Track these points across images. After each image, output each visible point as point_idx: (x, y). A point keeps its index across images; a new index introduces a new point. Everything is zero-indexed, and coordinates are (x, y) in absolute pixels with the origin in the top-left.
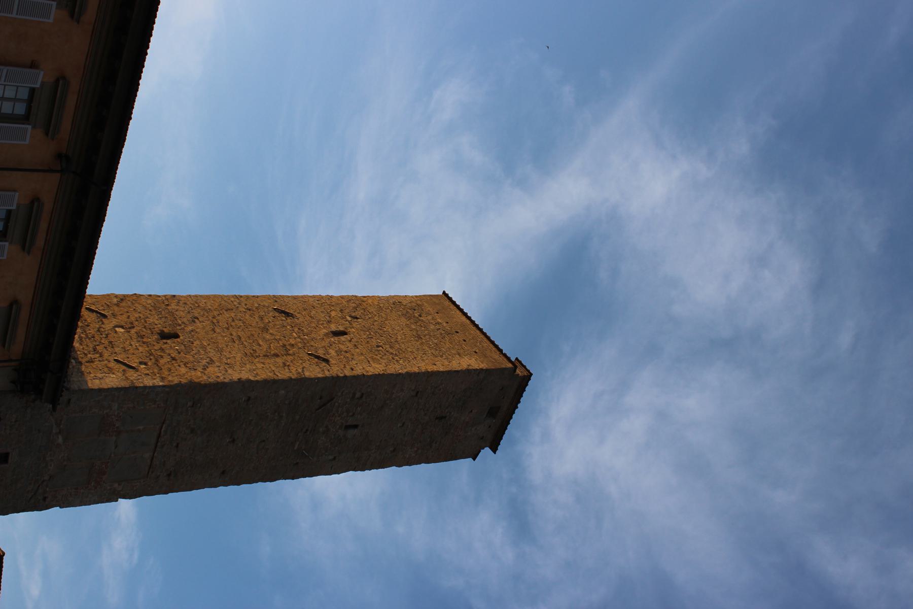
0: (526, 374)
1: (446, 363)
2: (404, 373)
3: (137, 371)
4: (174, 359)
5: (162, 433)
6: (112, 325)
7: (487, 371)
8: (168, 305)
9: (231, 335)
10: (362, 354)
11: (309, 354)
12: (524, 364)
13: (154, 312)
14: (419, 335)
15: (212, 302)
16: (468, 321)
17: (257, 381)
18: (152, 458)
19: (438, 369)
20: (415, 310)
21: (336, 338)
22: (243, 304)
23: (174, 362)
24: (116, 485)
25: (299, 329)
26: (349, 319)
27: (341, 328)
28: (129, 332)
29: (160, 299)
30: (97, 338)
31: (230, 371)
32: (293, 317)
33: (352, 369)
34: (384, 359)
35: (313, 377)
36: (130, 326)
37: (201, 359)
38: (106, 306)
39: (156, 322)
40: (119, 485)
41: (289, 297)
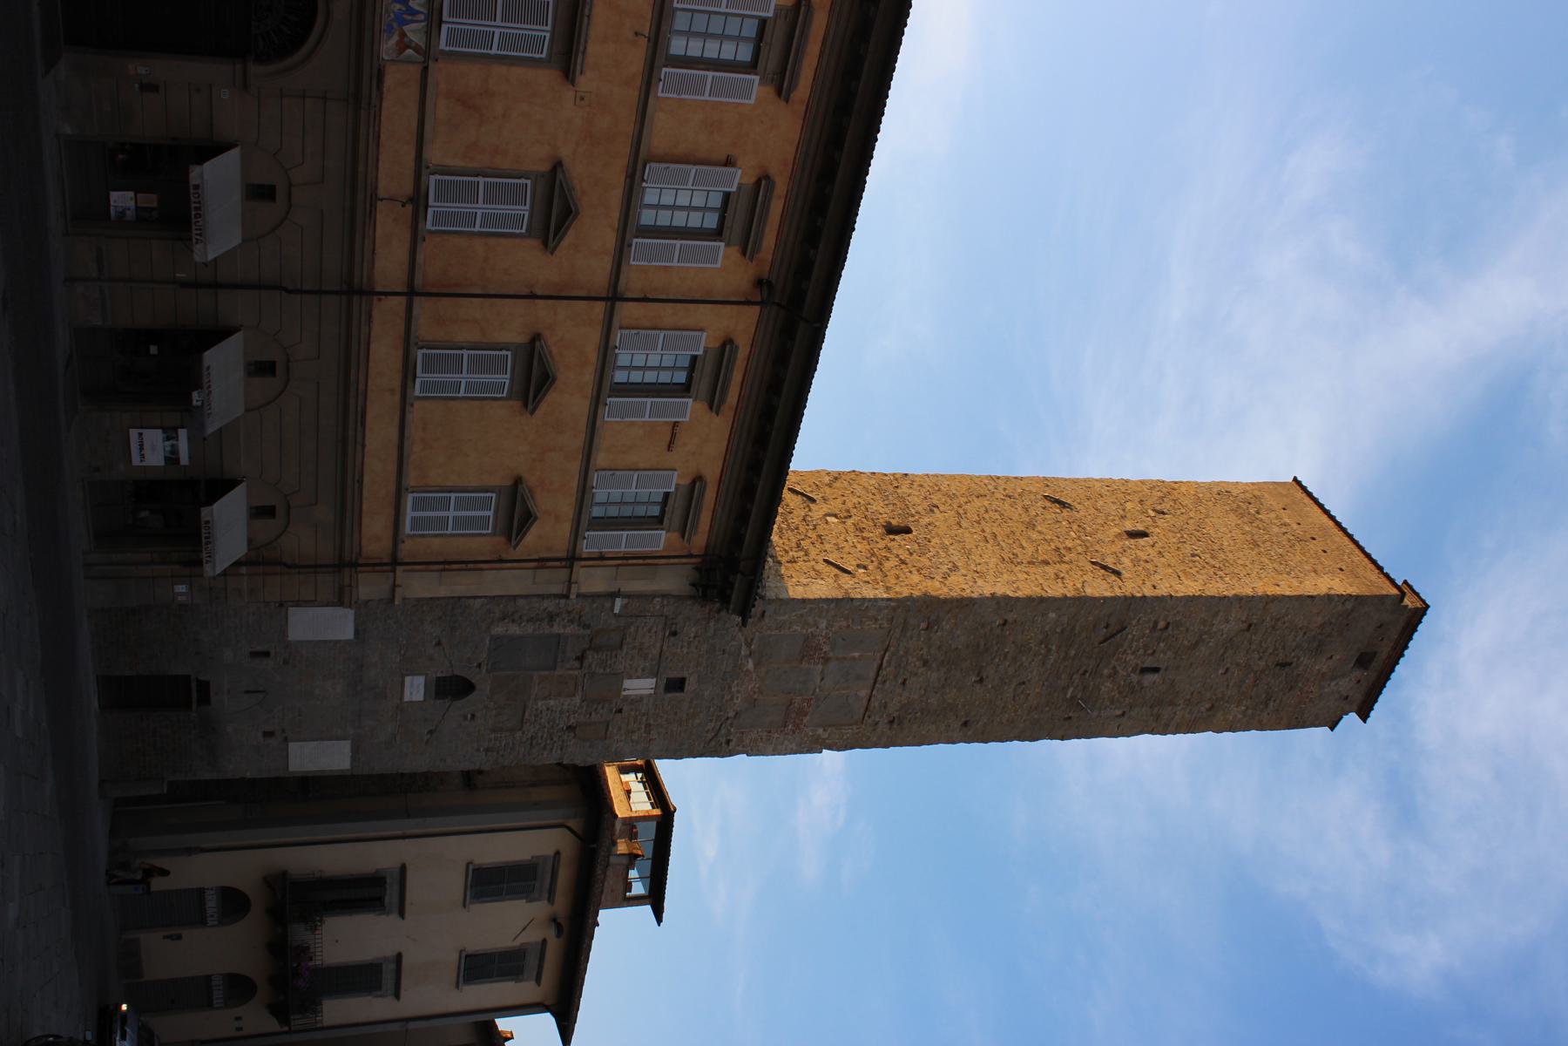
0: (1419, 606)
1: (1295, 583)
2: (1231, 595)
4: (903, 562)
5: (885, 664)
6: (821, 513)
7: (1358, 599)
8: (897, 487)
9: (983, 531)
10: (1169, 565)
11: (1093, 563)
13: (878, 496)
14: (1255, 541)
15: (959, 485)
16: (1331, 523)
17: (1018, 599)
18: (869, 700)
19: (1283, 593)
20: (1250, 503)
21: (1132, 541)
22: (1001, 489)
23: (903, 566)
24: (820, 731)
25: (1079, 526)
26: (1152, 514)
27: (1140, 527)
28: (844, 523)
29: (887, 478)
30: (802, 529)
31: (980, 582)
32: (1072, 509)
33: (1155, 587)
34: (1202, 574)
35: (1097, 595)
36: (845, 514)
37: (941, 563)
38: (814, 487)
39: (881, 511)
40: (824, 730)
41: (1066, 480)
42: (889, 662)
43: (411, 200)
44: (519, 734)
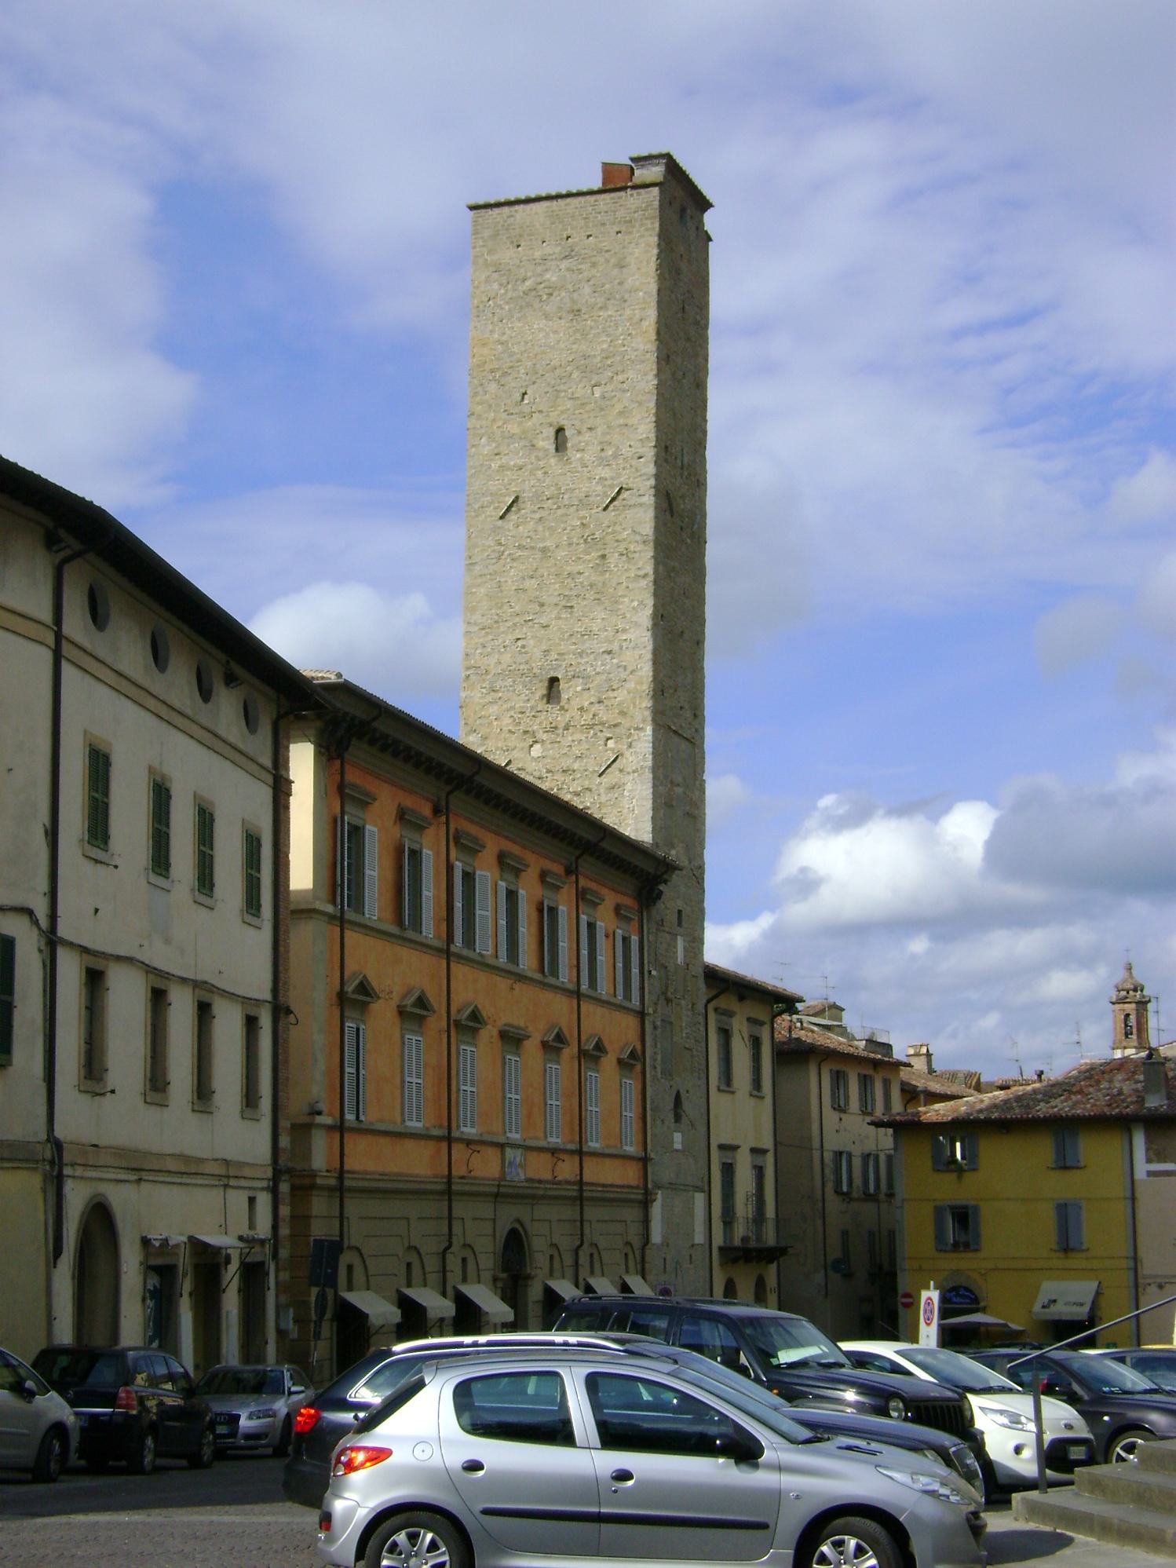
3: (622, 755)
12: (646, 154)
27: (551, 432)
29: (473, 677)
42: (675, 724)
43: (553, 1154)
44: (695, 1053)
